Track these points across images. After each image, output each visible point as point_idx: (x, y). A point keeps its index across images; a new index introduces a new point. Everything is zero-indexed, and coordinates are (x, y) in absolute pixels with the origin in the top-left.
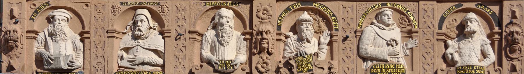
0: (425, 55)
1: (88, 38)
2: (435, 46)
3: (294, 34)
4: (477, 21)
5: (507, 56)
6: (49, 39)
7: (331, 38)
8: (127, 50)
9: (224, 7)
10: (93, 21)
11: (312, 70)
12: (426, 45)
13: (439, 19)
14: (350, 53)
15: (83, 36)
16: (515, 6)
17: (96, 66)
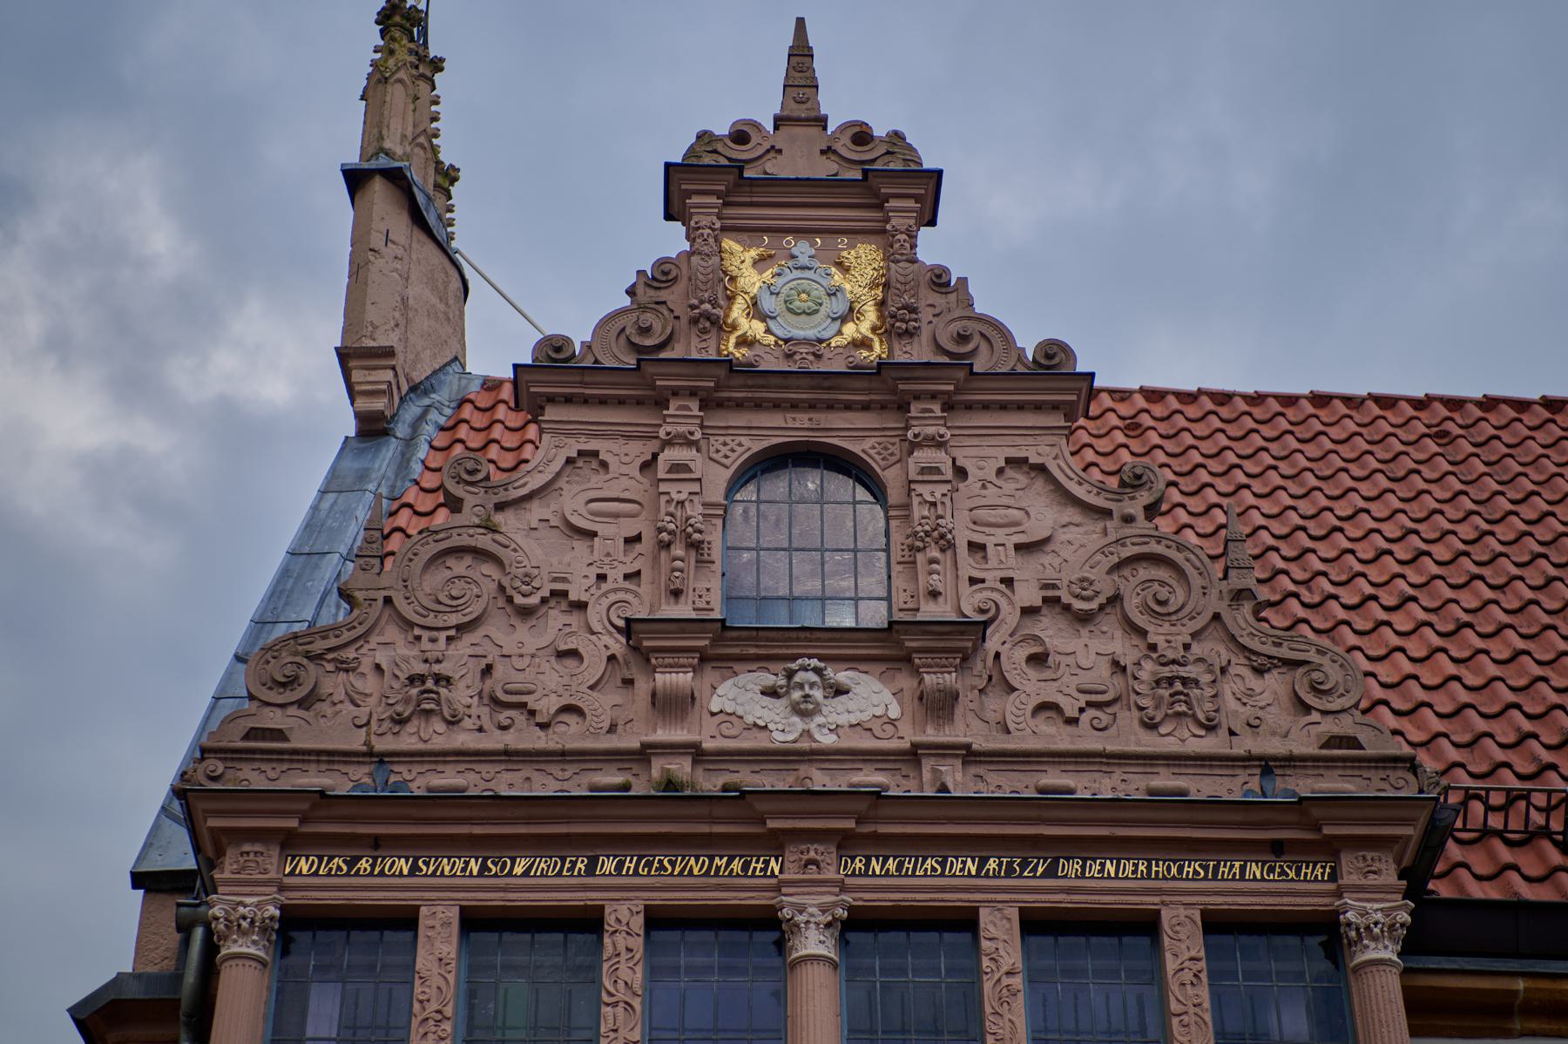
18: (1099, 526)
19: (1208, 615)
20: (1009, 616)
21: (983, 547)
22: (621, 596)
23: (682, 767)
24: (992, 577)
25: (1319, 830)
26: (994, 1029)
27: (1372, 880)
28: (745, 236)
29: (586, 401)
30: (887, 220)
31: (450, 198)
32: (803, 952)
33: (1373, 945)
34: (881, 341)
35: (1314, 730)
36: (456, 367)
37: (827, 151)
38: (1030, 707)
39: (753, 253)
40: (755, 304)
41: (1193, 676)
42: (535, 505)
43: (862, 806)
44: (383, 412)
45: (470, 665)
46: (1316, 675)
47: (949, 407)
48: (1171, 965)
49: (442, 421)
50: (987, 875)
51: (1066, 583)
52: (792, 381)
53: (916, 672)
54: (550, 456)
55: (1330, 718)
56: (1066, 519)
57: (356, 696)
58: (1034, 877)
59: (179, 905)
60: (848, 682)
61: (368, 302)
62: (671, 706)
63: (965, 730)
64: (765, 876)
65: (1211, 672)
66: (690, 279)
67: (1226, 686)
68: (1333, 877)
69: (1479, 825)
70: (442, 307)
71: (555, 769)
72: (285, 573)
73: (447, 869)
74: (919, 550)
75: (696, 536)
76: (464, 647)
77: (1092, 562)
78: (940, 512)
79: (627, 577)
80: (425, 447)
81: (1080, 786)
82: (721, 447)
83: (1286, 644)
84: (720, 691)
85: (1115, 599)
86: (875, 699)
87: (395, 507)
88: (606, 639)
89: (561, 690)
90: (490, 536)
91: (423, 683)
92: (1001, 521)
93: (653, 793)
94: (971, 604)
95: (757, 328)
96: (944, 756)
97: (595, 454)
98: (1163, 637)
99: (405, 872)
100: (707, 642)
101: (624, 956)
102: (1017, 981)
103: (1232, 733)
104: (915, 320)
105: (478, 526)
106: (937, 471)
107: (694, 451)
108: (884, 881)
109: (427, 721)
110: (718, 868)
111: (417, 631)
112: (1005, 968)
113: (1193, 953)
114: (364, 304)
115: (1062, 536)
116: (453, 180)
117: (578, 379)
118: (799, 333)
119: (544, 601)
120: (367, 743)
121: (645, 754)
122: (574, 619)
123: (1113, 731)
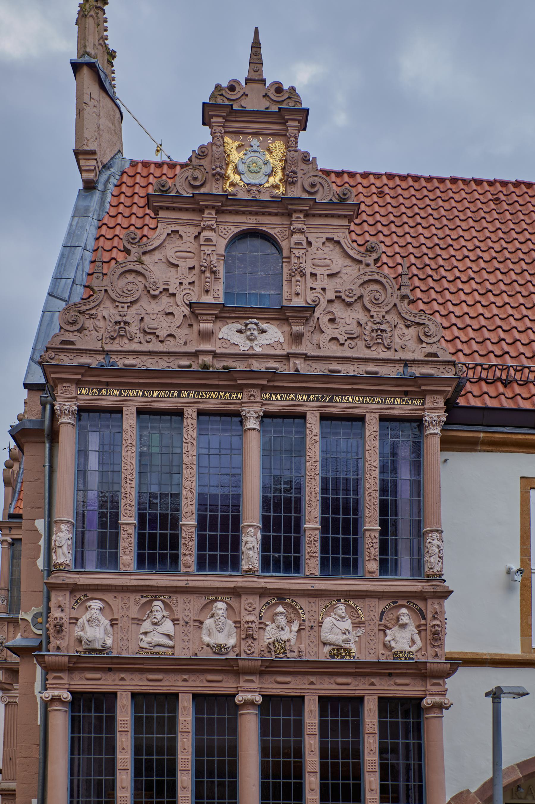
0: (370, 642)
1: (117, 624)
2: (377, 634)
3: (272, 623)
4: (408, 615)
5: (431, 644)
6: (86, 624)
7: (300, 626)
8: (145, 633)
9: (219, 601)
10: (120, 611)
11: (286, 653)
12: (370, 633)
13: (380, 613)
14: (314, 640)
15: (113, 622)
16: (436, 604)
17: (122, 647)
19: (392, 304)
20: (323, 303)
22: (188, 291)
23: (209, 359)
24: (318, 287)
25: (420, 387)
26: (309, 454)
27: (436, 405)
28: (233, 136)
29: (174, 209)
30: (287, 130)
31: (113, 66)
32: (249, 427)
33: (433, 428)
34: (283, 186)
35: (423, 350)
36: (119, 155)
37: (266, 96)
38: (328, 339)
40: (236, 167)
41: (384, 328)
42: (156, 252)
43: (269, 376)
44: (93, 180)
45: (136, 317)
46: (427, 329)
47: (306, 215)
48: (367, 433)
49: (115, 182)
50: (310, 401)
51: (344, 290)
52: (250, 204)
53: (290, 325)
54: (161, 233)
55: (429, 345)
56: (346, 264)
57: (97, 328)
58: (325, 402)
59: (41, 397)
60: (266, 328)
61: (85, 128)
62: (206, 336)
63: (305, 348)
64: (237, 399)
65: (391, 327)
66: (212, 156)
67: (396, 332)
68: (423, 404)
69: (478, 377)
70: (113, 127)
71: (166, 358)
72: (62, 255)
73: (131, 394)
74: (293, 276)
75: (214, 269)
76: (133, 310)
77: (353, 282)
78: (301, 261)
79: (190, 283)
80: (110, 196)
81: (343, 369)
82: (223, 231)
83: (418, 316)
84: (222, 330)
85: (361, 297)
86: (275, 335)
87: (100, 225)
88: (183, 309)
89: (167, 328)
90: (141, 265)
91: (120, 324)
92: (323, 264)
93: (200, 369)
94: (310, 297)
95: (236, 178)
96: (298, 357)
97: (177, 232)
98: (376, 313)
99: (118, 395)
100: (218, 312)
102: (317, 438)
103: (396, 350)
104: (296, 177)
105: (137, 261)
106: (301, 244)
107: (214, 233)
109: (122, 339)
110: (221, 396)
111: (117, 304)
112: (314, 434)
113: (375, 430)
114: (83, 129)
115: (344, 271)
116: (114, 57)
117: (171, 200)
118: (253, 181)
119: (161, 292)
120: (102, 347)
121: (196, 354)
122: (171, 300)
123: (355, 349)
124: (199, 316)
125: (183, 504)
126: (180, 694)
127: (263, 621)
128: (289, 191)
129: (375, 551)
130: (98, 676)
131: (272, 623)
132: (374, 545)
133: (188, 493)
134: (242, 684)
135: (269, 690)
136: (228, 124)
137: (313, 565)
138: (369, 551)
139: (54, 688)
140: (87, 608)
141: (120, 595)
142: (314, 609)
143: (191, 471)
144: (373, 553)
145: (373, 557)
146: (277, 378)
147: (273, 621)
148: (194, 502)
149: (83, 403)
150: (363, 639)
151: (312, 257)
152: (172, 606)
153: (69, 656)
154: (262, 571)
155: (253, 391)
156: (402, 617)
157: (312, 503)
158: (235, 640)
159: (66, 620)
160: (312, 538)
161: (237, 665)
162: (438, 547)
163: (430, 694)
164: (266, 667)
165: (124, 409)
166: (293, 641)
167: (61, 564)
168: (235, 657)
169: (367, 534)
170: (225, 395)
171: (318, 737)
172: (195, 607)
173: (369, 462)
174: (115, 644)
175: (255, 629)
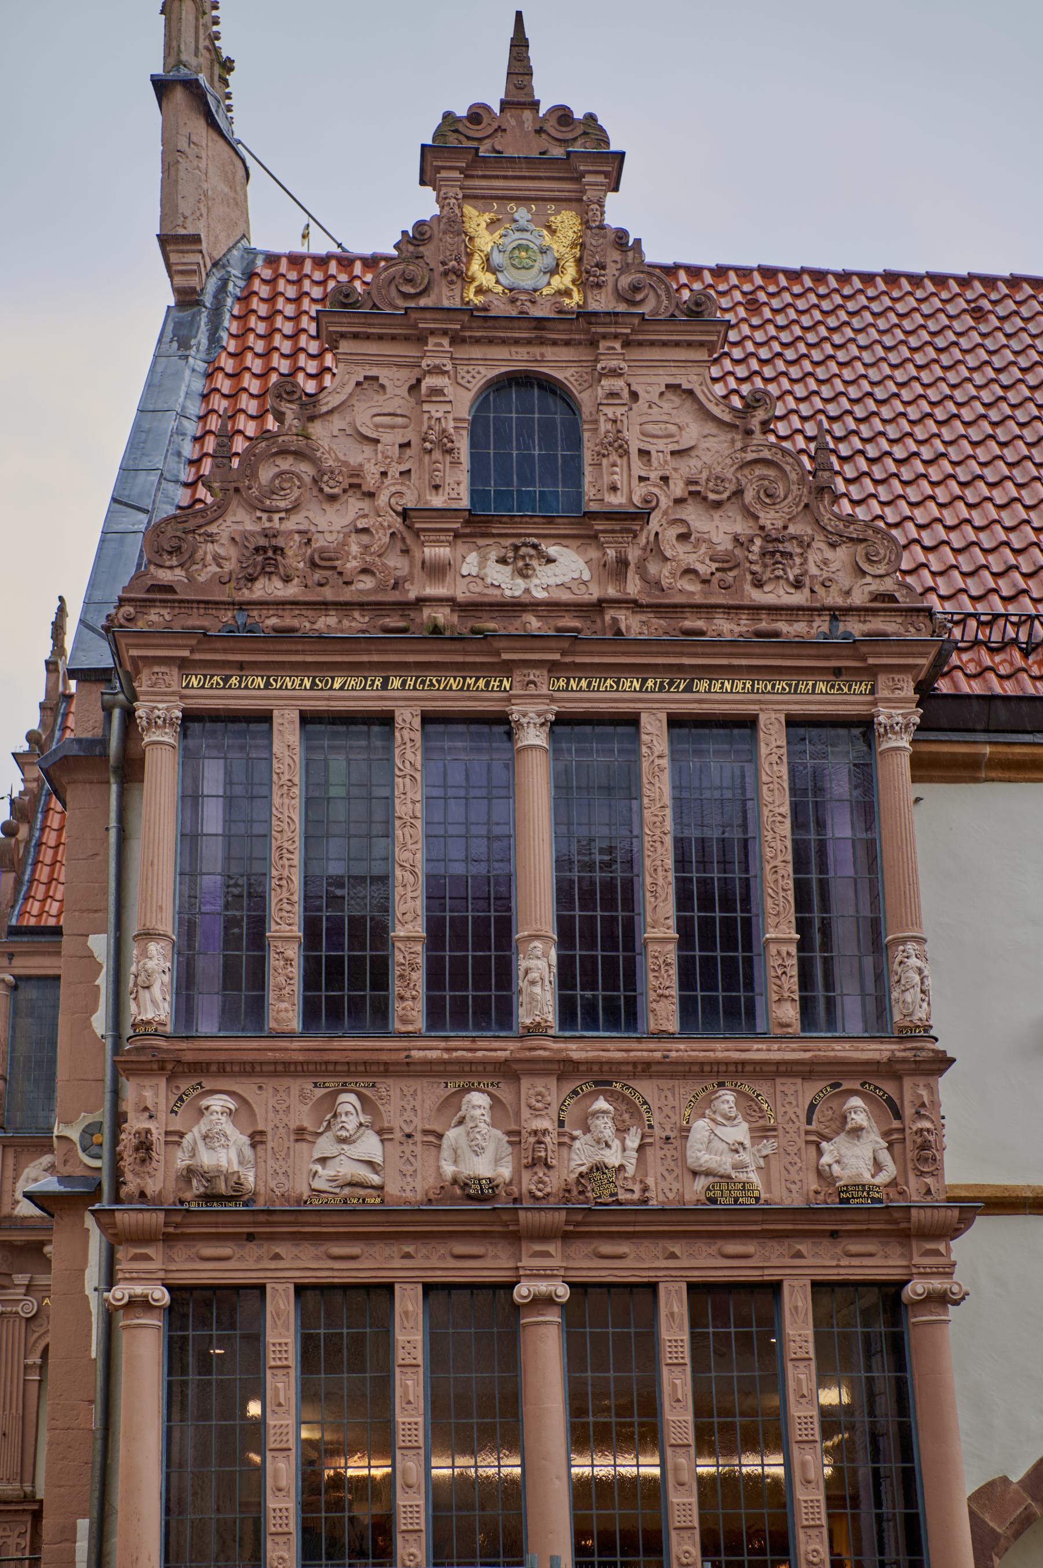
0: (789, 1167)
1: (262, 1142)
2: (803, 1151)
3: (584, 1134)
5: (916, 1168)
6: (201, 1144)
7: (642, 1139)
8: (323, 1160)
10: (271, 1115)
11: (616, 1194)
12: (789, 1149)
15: (257, 1139)
18: (729, 436)
21: (648, 453)
23: (442, 615)
24: (654, 476)
25: (865, 660)
26: (649, 793)
28: (480, 203)
29: (368, 337)
30: (583, 192)
32: (526, 743)
33: (894, 737)
35: (867, 589)
39: (487, 217)
47: (627, 344)
48: (764, 750)
52: (516, 324)
53: (601, 547)
55: (878, 580)
56: (706, 432)
62: (437, 570)
68: (872, 692)
74: (604, 456)
79: (401, 473)
84: (468, 560)
85: (739, 493)
86: (573, 566)
91: (265, 552)
94: (639, 492)
95: (486, 279)
101: (409, 744)
102: (665, 762)
108: (578, 695)
111: (259, 514)
112: (656, 754)
113: (779, 743)
115: (704, 444)
117: (362, 320)
122: (365, 505)
124: (422, 534)
125: (397, 898)
126: (397, 1286)
127: (567, 1129)
128: (590, 300)
129: (791, 983)
130: (225, 1251)
131: (584, 1134)
132: (788, 970)
133: (407, 874)
134: (526, 1262)
135: (584, 1273)
136: (469, 183)
137: (664, 1014)
138: (778, 982)
139: (132, 1279)
140: (201, 1112)
141: (270, 1083)
142: (671, 1102)
143: (412, 831)
144: (786, 986)
145: (786, 995)
146: (580, 648)
147: (587, 1130)
148: (418, 893)
149: (193, 704)
150: (775, 1165)
151: (640, 420)
152: (378, 1103)
153: (166, 1210)
154: (561, 1029)
155: (533, 674)
156: (853, 1116)
157: (659, 889)
158: (510, 1169)
159: (157, 1135)
160: (661, 960)
161: (517, 1222)
162: (920, 971)
163: (920, 1274)
164: (578, 1224)
165: (276, 713)
166: (631, 1170)
167: (149, 1023)
168: (511, 1206)
169: (773, 949)
170: (476, 682)
171: (688, 1369)
172: (426, 1106)
173: (771, 807)
174: (261, 1184)
175: (550, 1147)
